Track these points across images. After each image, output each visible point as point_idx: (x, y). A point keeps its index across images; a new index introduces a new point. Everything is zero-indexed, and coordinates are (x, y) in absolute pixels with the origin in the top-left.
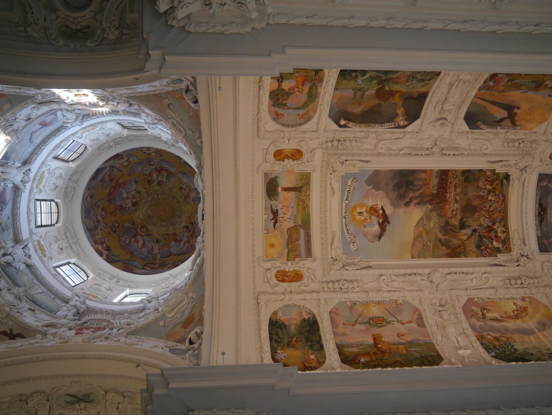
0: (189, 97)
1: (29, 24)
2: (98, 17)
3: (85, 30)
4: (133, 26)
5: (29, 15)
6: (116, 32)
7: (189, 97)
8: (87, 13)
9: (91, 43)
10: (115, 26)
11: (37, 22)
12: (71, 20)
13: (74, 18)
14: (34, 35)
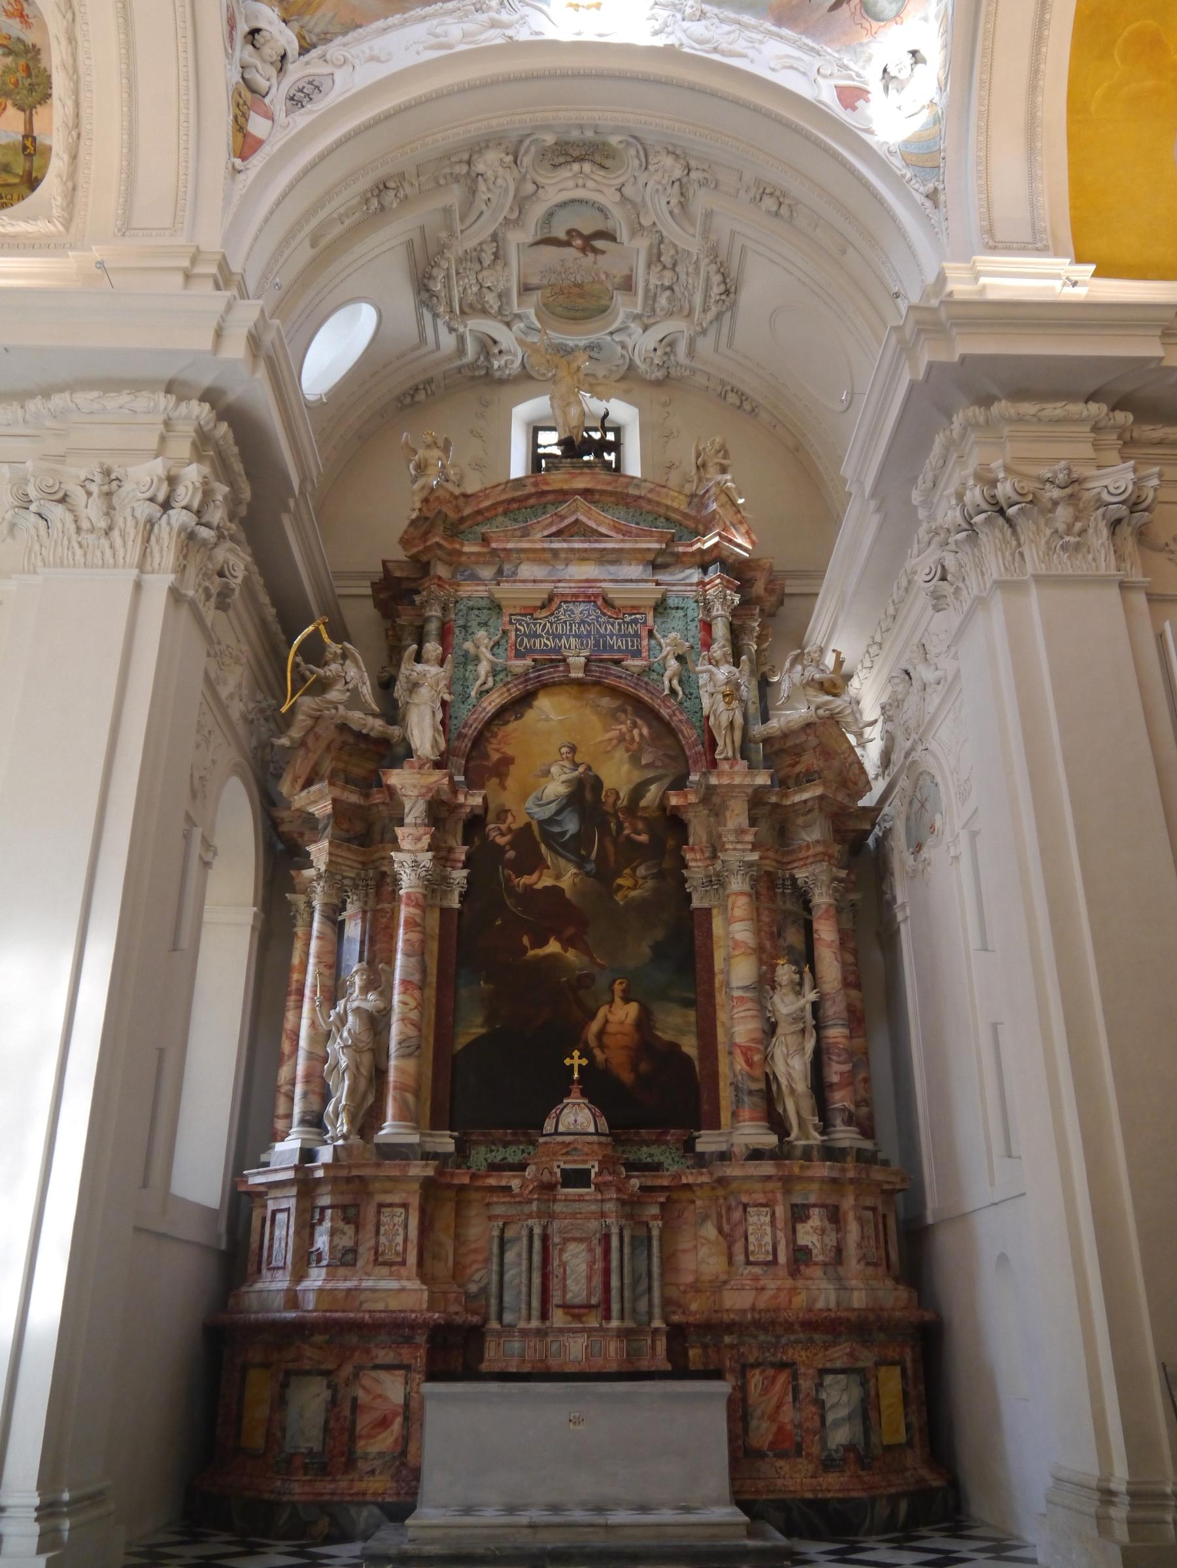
0: (272, 49)
1: (677, 184)
2: (530, 188)
3: (562, 159)
4: (442, 181)
5: (674, 201)
6: (480, 167)
7: (272, 49)
8: (552, 196)
9: (544, 141)
10: (485, 180)
11: (660, 187)
12: (590, 184)
13: (584, 186)
14: (669, 161)
